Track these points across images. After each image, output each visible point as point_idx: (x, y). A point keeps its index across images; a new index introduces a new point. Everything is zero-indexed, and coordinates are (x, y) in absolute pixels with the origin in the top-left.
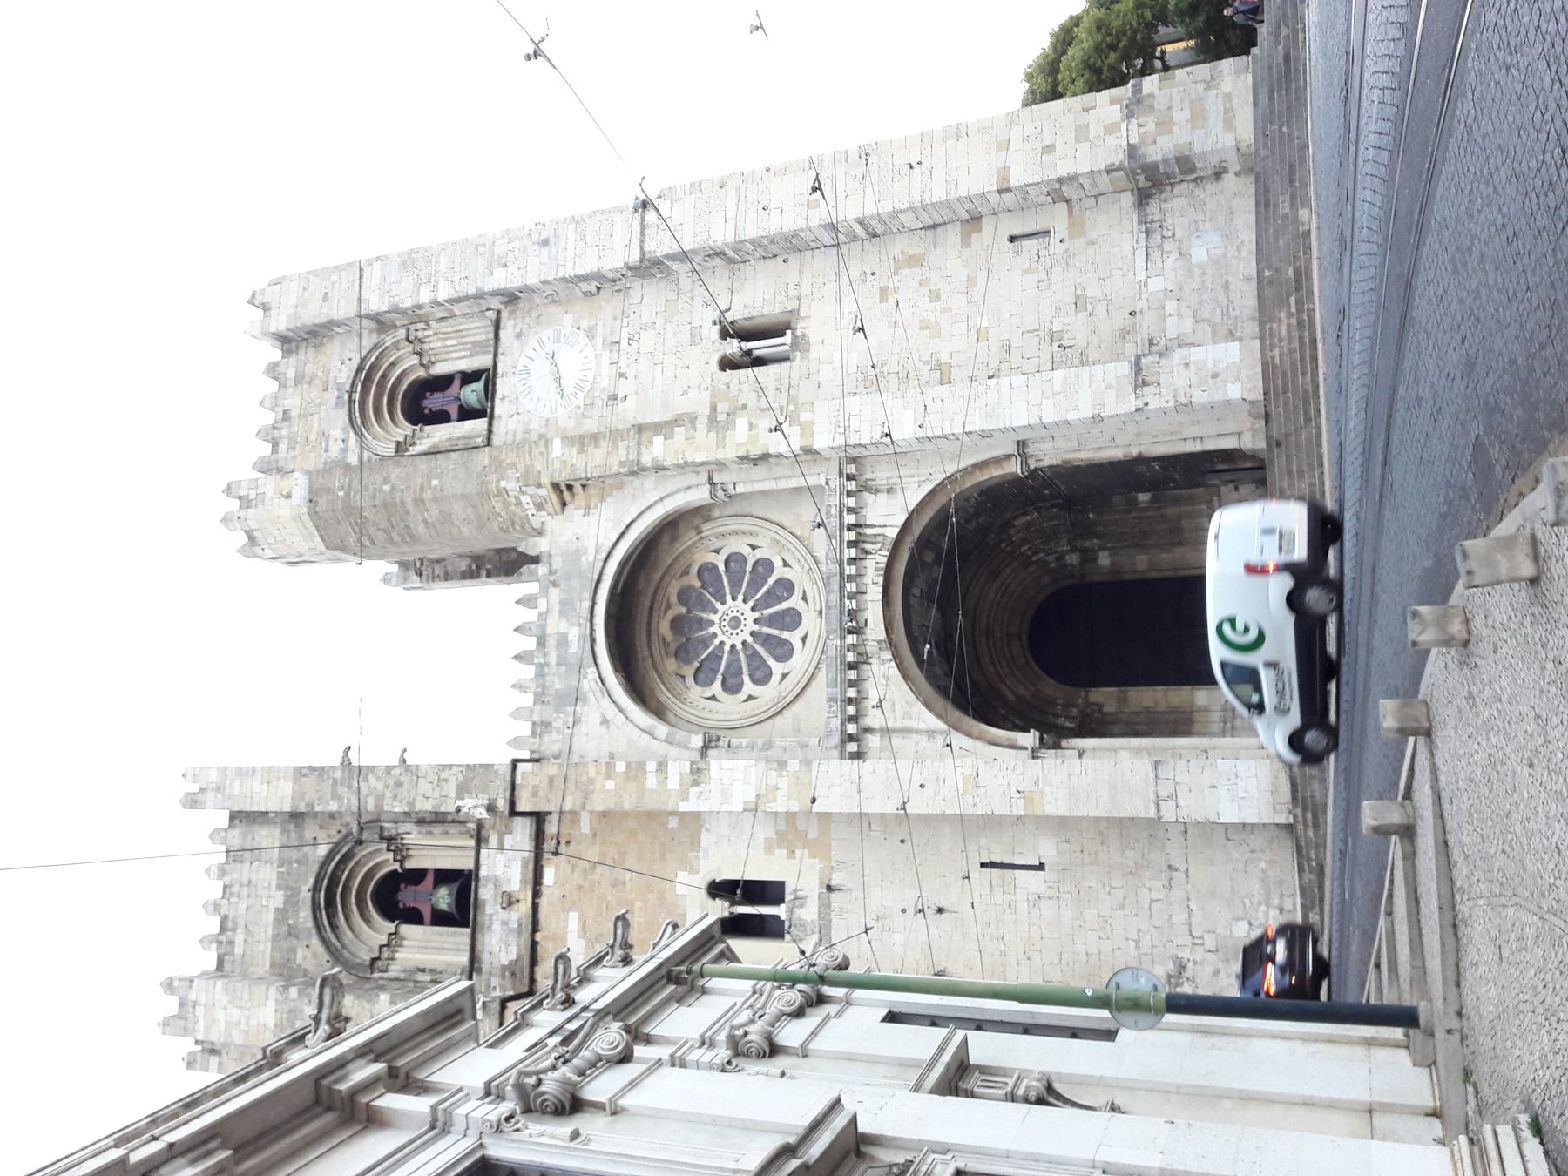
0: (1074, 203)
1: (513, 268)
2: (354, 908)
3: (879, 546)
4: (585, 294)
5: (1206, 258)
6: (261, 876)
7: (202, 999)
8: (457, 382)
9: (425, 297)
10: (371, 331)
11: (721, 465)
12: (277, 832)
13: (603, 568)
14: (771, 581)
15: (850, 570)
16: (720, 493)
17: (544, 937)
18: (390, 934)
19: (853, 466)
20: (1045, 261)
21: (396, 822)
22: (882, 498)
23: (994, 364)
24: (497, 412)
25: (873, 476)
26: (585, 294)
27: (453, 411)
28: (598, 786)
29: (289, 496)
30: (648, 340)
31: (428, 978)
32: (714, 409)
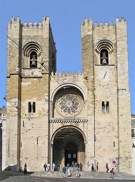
10: (115, 42)
12: (41, 35)
22: (82, 125)
30: (108, 90)
32: (97, 101)
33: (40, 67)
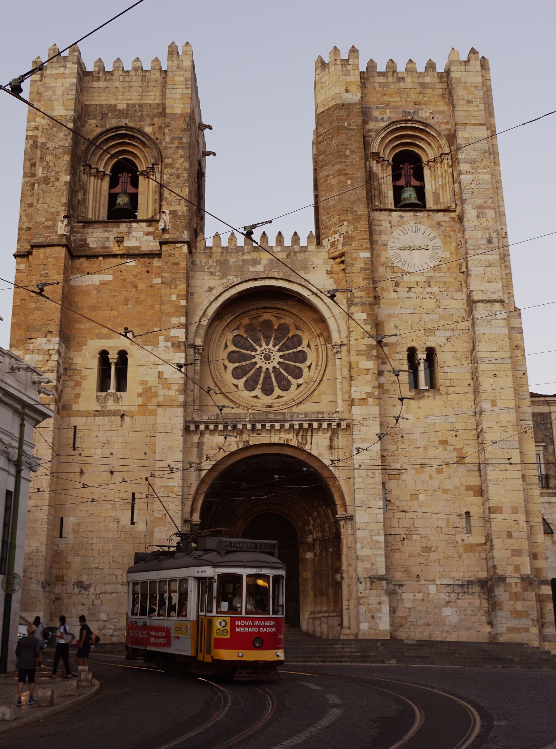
0: (485, 547)
1: (476, 222)
2: (117, 150)
3: (300, 441)
4: (461, 265)
5: (444, 615)
6: (134, 94)
7: (67, 71)
8: (418, 184)
9: (464, 167)
10: (449, 130)
11: (349, 351)
12: (158, 101)
13: (297, 283)
14: (290, 378)
15: (287, 426)
16: (335, 350)
17: (100, 262)
18: (104, 172)
19: (345, 427)
20: (452, 531)
21: (161, 172)
22: (327, 442)
23: (397, 503)
24: (394, 214)
25: (340, 437)
26: (461, 265)
27: (401, 182)
28: (173, 290)
29: (347, 91)
30: (430, 304)
31: (80, 198)
33: (150, 216)
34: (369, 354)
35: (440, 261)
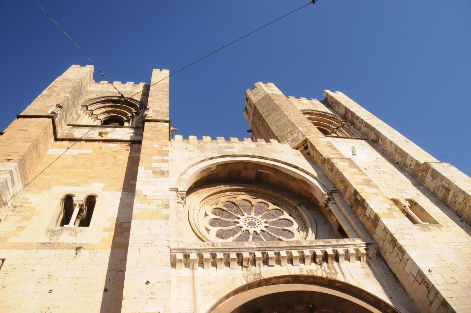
1: (390, 135)
17: (82, 144)
34: (368, 184)
35: (376, 158)
